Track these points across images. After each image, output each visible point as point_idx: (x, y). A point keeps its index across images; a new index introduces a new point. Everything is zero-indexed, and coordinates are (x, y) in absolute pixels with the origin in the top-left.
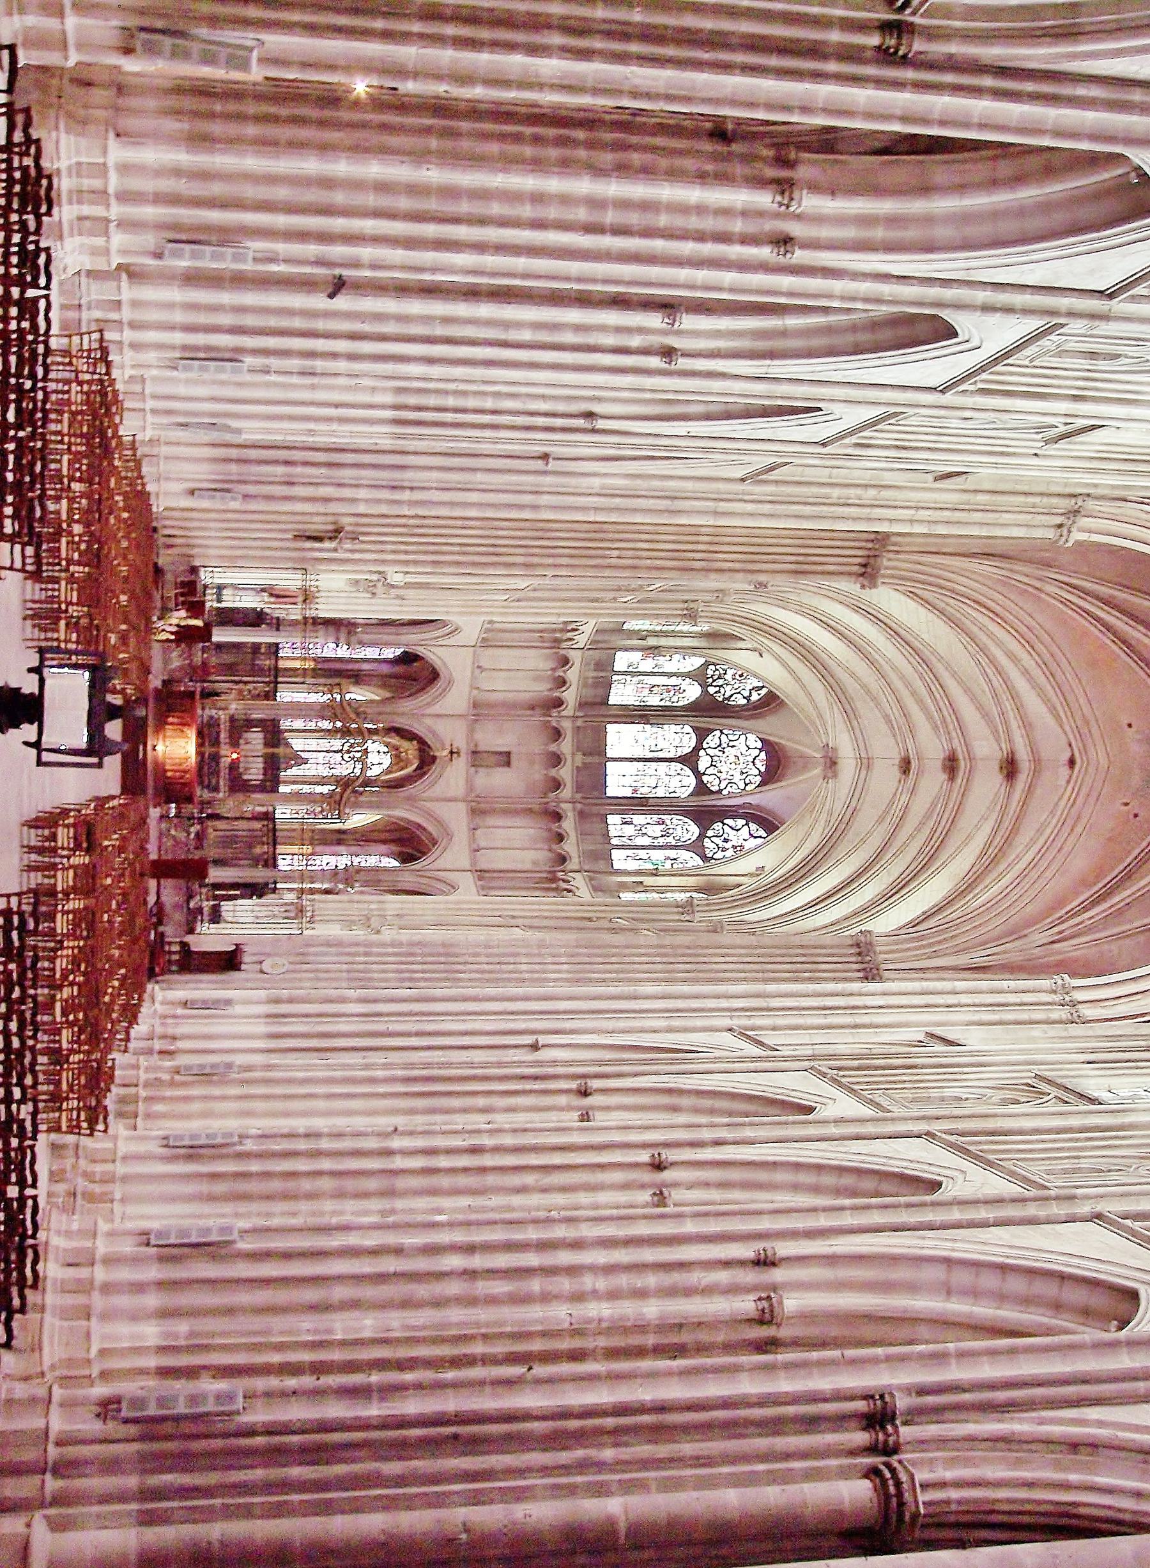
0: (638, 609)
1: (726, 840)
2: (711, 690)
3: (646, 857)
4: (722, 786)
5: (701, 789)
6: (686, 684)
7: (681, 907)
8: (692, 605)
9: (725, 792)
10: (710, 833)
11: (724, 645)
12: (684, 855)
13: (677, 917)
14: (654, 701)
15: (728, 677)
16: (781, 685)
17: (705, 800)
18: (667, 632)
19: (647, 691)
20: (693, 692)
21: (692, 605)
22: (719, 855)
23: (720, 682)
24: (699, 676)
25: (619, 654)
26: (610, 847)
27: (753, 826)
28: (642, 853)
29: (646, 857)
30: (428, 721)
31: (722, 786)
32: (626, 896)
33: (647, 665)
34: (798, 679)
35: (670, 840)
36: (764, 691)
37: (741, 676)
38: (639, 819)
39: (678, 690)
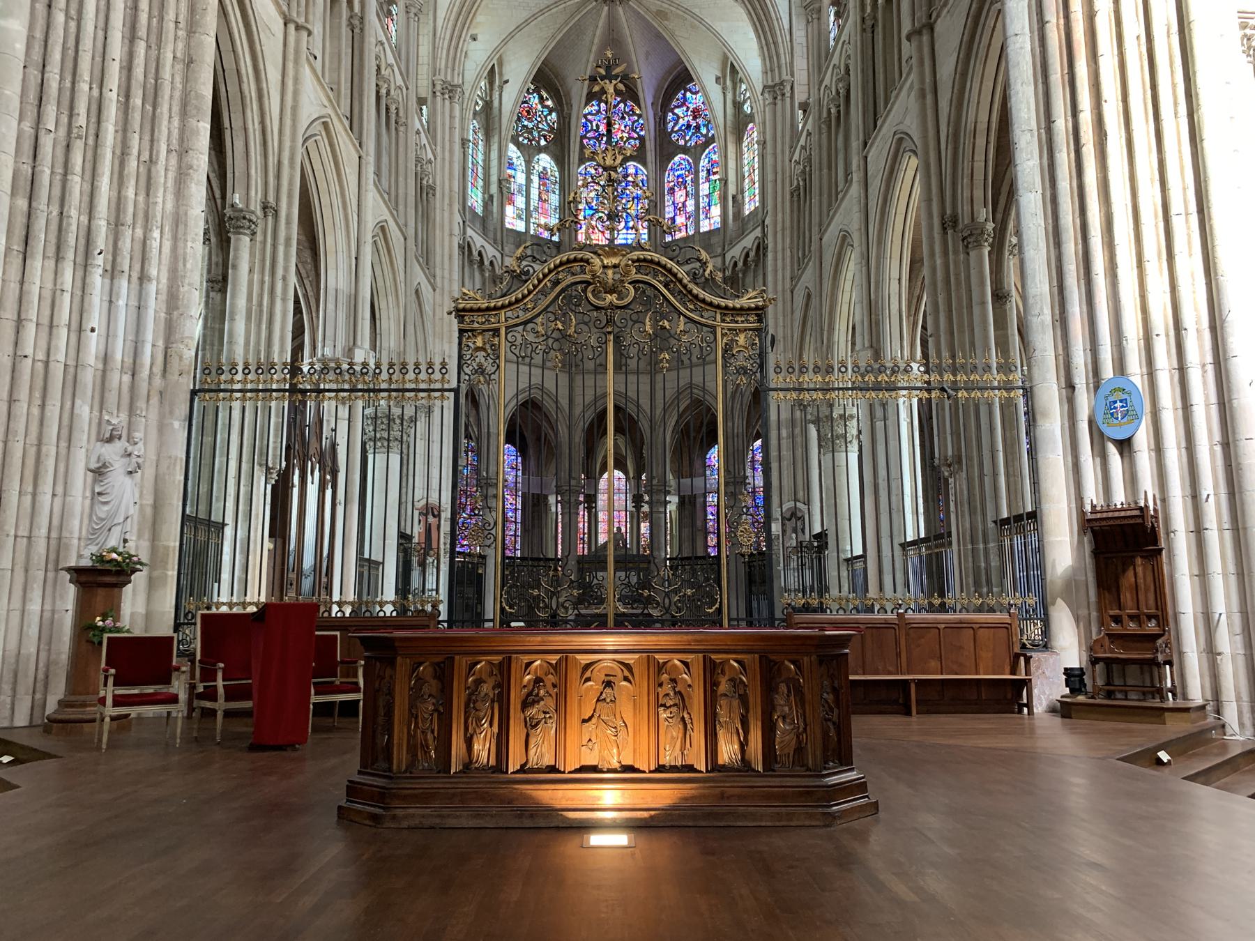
0: (443, 148)
1: (689, 126)
2: (543, 143)
3: (706, 200)
4: (636, 136)
5: (640, 156)
6: (538, 169)
7: (775, 98)
8: (438, 87)
9: (642, 133)
10: (682, 142)
11: (497, 119)
12: (704, 162)
13: (788, 100)
14: (554, 199)
15: (530, 125)
16: (535, 54)
17: (650, 146)
18: (484, 174)
19: (546, 206)
20: (545, 161)
21: (438, 87)
22: (704, 131)
23: (535, 134)
24: (529, 152)
25: (508, 226)
26: (697, 236)
27: (675, 103)
28: (703, 203)
29: (706, 200)
30: (578, 410)
31: (636, 136)
32: (750, 205)
33: (520, 201)
34: (527, 22)
35: (689, 179)
36: (545, 95)
37: (528, 112)
38: (669, 212)
39: (543, 176)
